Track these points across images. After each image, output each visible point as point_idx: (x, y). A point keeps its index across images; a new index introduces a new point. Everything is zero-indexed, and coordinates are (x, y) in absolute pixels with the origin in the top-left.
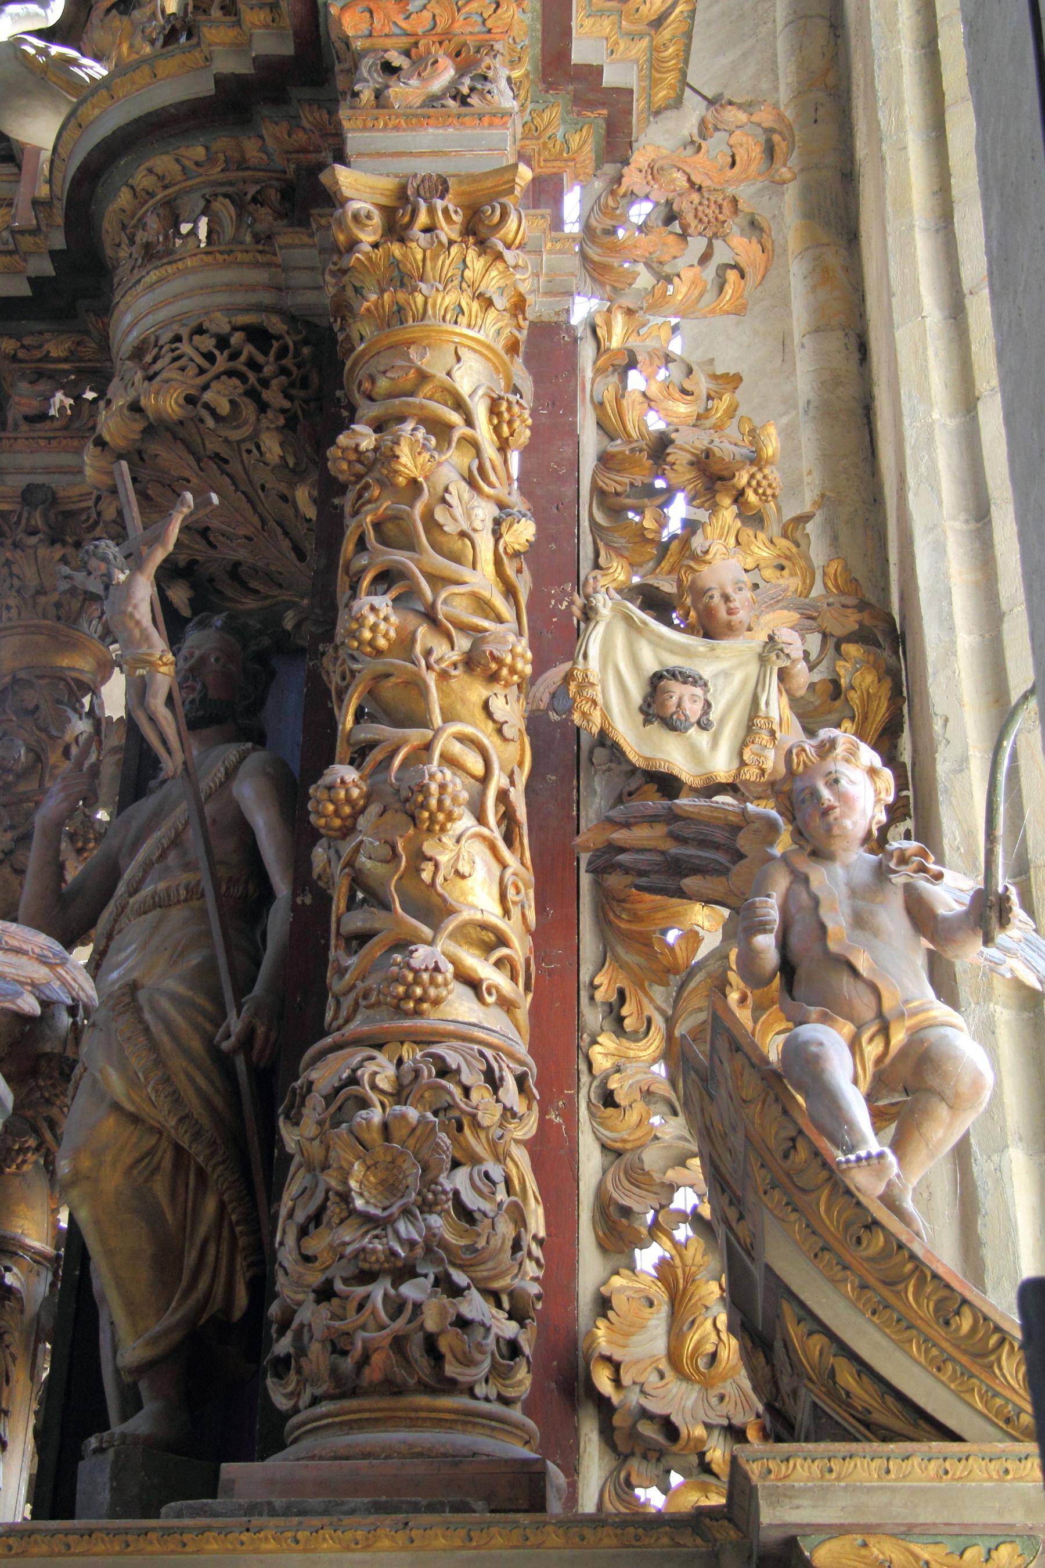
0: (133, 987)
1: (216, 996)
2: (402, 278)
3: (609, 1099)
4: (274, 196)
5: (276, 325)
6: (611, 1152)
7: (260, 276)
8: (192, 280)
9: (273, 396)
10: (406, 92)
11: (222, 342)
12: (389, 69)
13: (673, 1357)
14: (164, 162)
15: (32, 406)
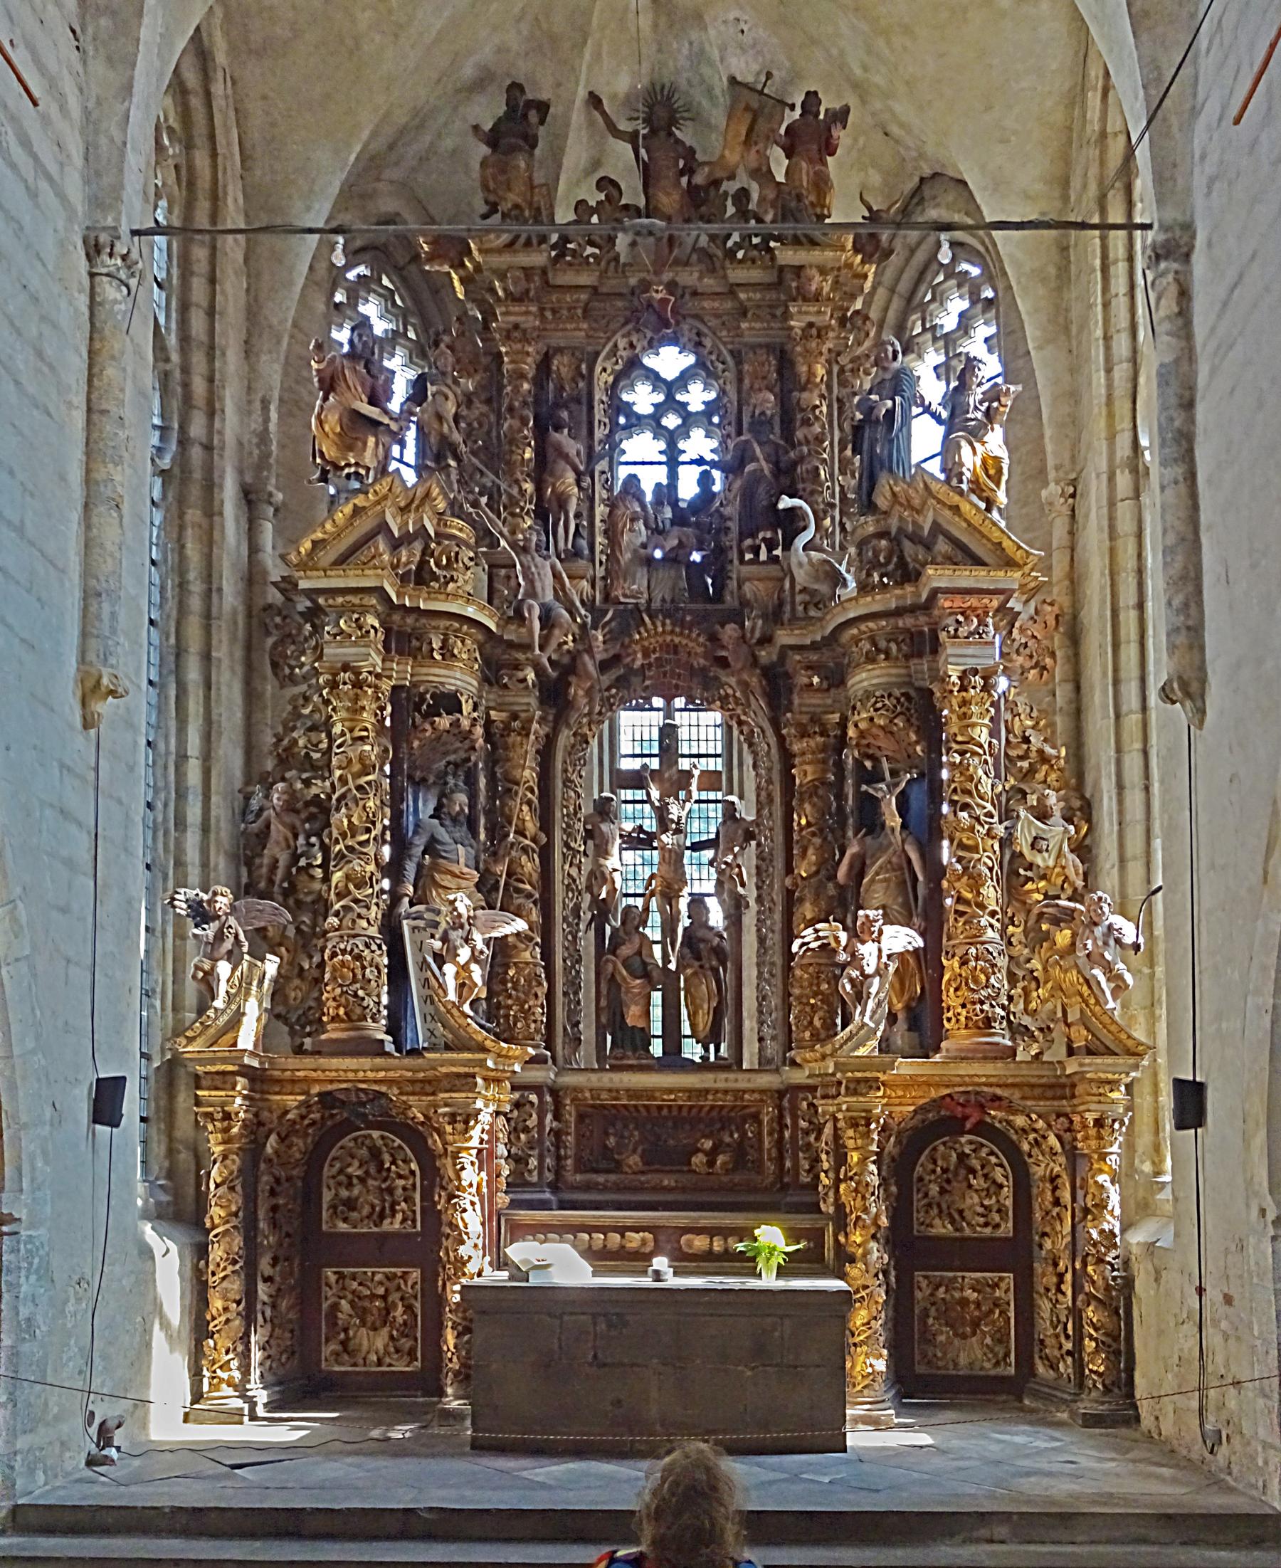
5: (913, 693)
7: (903, 671)
9: (913, 720)
11: (898, 700)
14: (871, 625)
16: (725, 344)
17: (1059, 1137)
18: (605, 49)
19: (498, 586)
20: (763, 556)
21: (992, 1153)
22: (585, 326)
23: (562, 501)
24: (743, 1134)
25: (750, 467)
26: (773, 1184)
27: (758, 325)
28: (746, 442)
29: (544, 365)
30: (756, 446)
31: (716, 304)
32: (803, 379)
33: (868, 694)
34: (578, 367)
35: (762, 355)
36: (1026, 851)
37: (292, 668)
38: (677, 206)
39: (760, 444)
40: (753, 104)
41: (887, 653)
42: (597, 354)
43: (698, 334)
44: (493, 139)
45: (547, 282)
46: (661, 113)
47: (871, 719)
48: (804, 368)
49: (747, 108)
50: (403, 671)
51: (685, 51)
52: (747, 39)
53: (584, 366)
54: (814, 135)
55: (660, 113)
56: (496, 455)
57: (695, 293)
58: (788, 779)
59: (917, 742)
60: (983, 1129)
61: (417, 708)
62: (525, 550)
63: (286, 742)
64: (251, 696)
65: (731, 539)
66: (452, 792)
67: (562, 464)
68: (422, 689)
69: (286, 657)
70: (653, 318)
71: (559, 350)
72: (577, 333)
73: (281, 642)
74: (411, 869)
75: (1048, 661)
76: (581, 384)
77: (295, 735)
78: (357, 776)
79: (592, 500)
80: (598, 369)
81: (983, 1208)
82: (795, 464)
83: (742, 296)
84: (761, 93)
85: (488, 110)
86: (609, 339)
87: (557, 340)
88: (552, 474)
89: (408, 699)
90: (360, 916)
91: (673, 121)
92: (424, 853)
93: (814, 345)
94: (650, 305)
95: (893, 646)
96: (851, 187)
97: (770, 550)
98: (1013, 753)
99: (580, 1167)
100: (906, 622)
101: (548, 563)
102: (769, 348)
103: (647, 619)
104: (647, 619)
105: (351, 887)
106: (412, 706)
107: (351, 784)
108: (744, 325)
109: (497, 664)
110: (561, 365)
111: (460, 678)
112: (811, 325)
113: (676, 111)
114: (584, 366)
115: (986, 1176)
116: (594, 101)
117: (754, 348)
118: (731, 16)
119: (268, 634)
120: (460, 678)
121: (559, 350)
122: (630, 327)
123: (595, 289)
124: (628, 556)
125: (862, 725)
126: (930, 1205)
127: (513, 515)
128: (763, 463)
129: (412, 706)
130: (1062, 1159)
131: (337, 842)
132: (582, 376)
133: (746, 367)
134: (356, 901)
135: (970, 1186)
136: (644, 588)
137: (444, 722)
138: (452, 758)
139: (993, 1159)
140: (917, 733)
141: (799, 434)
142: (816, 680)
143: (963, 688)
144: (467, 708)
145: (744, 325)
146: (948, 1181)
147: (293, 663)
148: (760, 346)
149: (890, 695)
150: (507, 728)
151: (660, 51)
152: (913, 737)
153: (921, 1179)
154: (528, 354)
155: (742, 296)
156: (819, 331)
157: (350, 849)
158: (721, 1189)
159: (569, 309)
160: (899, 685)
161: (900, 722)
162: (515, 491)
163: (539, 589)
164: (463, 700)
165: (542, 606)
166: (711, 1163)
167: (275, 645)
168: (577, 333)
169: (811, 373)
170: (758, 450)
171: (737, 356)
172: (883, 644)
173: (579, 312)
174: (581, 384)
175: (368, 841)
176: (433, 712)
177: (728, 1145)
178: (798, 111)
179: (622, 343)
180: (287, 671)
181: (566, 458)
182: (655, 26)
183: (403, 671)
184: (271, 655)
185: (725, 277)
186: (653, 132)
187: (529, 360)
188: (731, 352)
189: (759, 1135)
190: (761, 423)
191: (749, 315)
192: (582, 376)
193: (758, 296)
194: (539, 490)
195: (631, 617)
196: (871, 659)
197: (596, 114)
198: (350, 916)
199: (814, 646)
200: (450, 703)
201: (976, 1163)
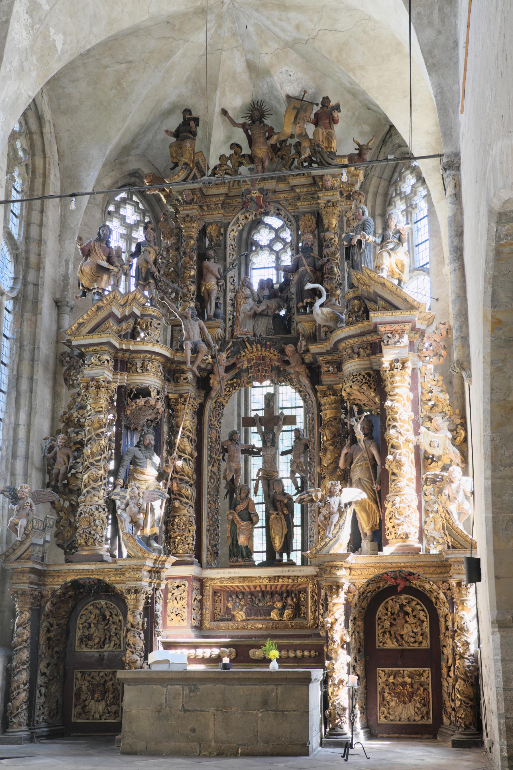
0: (360, 479)
1: (372, 480)
2: (393, 376)
3: (425, 495)
4: (369, 347)
5: (372, 373)
6: (426, 502)
7: (368, 362)
8: (357, 363)
9: (372, 386)
10: (391, 341)
11: (364, 376)
12: (388, 337)
13: (434, 528)
14: (351, 341)
15: (326, 369)
16: (290, 213)
17: (445, 593)
18: (227, 89)
19: (175, 335)
21: (418, 604)
22: (222, 211)
23: (209, 292)
24: (299, 600)
25: (301, 269)
26: (313, 625)
27: (305, 203)
28: (299, 257)
29: (203, 232)
30: (303, 259)
31: (286, 195)
32: (326, 226)
33: (350, 374)
34: (220, 231)
35: (308, 217)
38: (265, 154)
39: (306, 258)
40: (298, 105)
41: (359, 354)
42: (229, 223)
43: (278, 210)
44: (177, 134)
45: (203, 194)
46: (256, 113)
47: (351, 387)
48: (327, 221)
49: (294, 108)
50: (123, 379)
51: (265, 86)
52: (293, 78)
53: (222, 230)
54: (327, 115)
55: (256, 115)
56: (178, 276)
57: (275, 192)
59: (375, 396)
60: (410, 590)
61: (129, 396)
62: (186, 318)
63: (67, 415)
64: (55, 395)
66: (145, 434)
67: (210, 275)
68: (131, 387)
69: (70, 376)
70: (254, 205)
71: (211, 224)
72: (217, 215)
73: (69, 369)
76: (221, 238)
77: (72, 411)
78: (95, 429)
79: (225, 291)
80: (229, 230)
81: (413, 632)
82: (322, 266)
83: (298, 191)
84: (302, 100)
85: (175, 122)
86: (235, 216)
87: (209, 219)
90: (94, 495)
91: (262, 115)
93: (331, 210)
94: (251, 199)
95: (361, 350)
96: (345, 138)
99: (214, 618)
100: (368, 338)
101: (197, 323)
102: (312, 213)
103: (248, 345)
104: (248, 345)
105: (91, 481)
106: (126, 396)
107: (93, 433)
108: (299, 204)
109: (172, 372)
110: (212, 230)
111: (152, 380)
112: (329, 201)
113: (264, 112)
114: (222, 230)
115: (415, 616)
116: (224, 112)
117: (304, 214)
118: (284, 69)
119: (63, 365)
121: (211, 224)
122: (244, 210)
123: (227, 194)
125: (348, 390)
126: (384, 633)
127: (184, 301)
128: (307, 267)
129: (126, 396)
130: (447, 605)
132: (222, 234)
133: (300, 223)
134: (93, 488)
135: (406, 622)
137: (141, 401)
139: (419, 607)
140: (374, 392)
141: (325, 252)
143: (392, 369)
144: (153, 394)
145: (299, 204)
146: (395, 619)
147: (74, 378)
148: (307, 213)
149: (360, 374)
151: (254, 87)
152: (373, 394)
153: (380, 619)
154: (193, 227)
155: (298, 191)
156: (333, 203)
157: (92, 464)
158: (286, 627)
159: (215, 205)
160: (365, 369)
161: (364, 387)
162: (185, 290)
163: (192, 336)
164: (152, 390)
166: (281, 615)
167: (67, 370)
168: (217, 215)
169: (330, 223)
170: (304, 261)
171: (296, 218)
172: (356, 350)
173: (220, 205)
174: (221, 238)
175: (100, 459)
176: (136, 397)
177: (291, 605)
178: (320, 106)
179: (241, 217)
180: (71, 382)
181: (211, 272)
182: (251, 77)
183: (123, 379)
184: (64, 375)
185: (289, 183)
186: (254, 122)
187: (194, 230)
188: (294, 216)
189: (306, 600)
190: (307, 248)
191: (301, 199)
192: (222, 234)
193: (305, 190)
195: (240, 345)
196: (351, 357)
197: (226, 118)
198: (90, 495)
199: (328, 353)
200: (145, 392)
201: (409, 609)
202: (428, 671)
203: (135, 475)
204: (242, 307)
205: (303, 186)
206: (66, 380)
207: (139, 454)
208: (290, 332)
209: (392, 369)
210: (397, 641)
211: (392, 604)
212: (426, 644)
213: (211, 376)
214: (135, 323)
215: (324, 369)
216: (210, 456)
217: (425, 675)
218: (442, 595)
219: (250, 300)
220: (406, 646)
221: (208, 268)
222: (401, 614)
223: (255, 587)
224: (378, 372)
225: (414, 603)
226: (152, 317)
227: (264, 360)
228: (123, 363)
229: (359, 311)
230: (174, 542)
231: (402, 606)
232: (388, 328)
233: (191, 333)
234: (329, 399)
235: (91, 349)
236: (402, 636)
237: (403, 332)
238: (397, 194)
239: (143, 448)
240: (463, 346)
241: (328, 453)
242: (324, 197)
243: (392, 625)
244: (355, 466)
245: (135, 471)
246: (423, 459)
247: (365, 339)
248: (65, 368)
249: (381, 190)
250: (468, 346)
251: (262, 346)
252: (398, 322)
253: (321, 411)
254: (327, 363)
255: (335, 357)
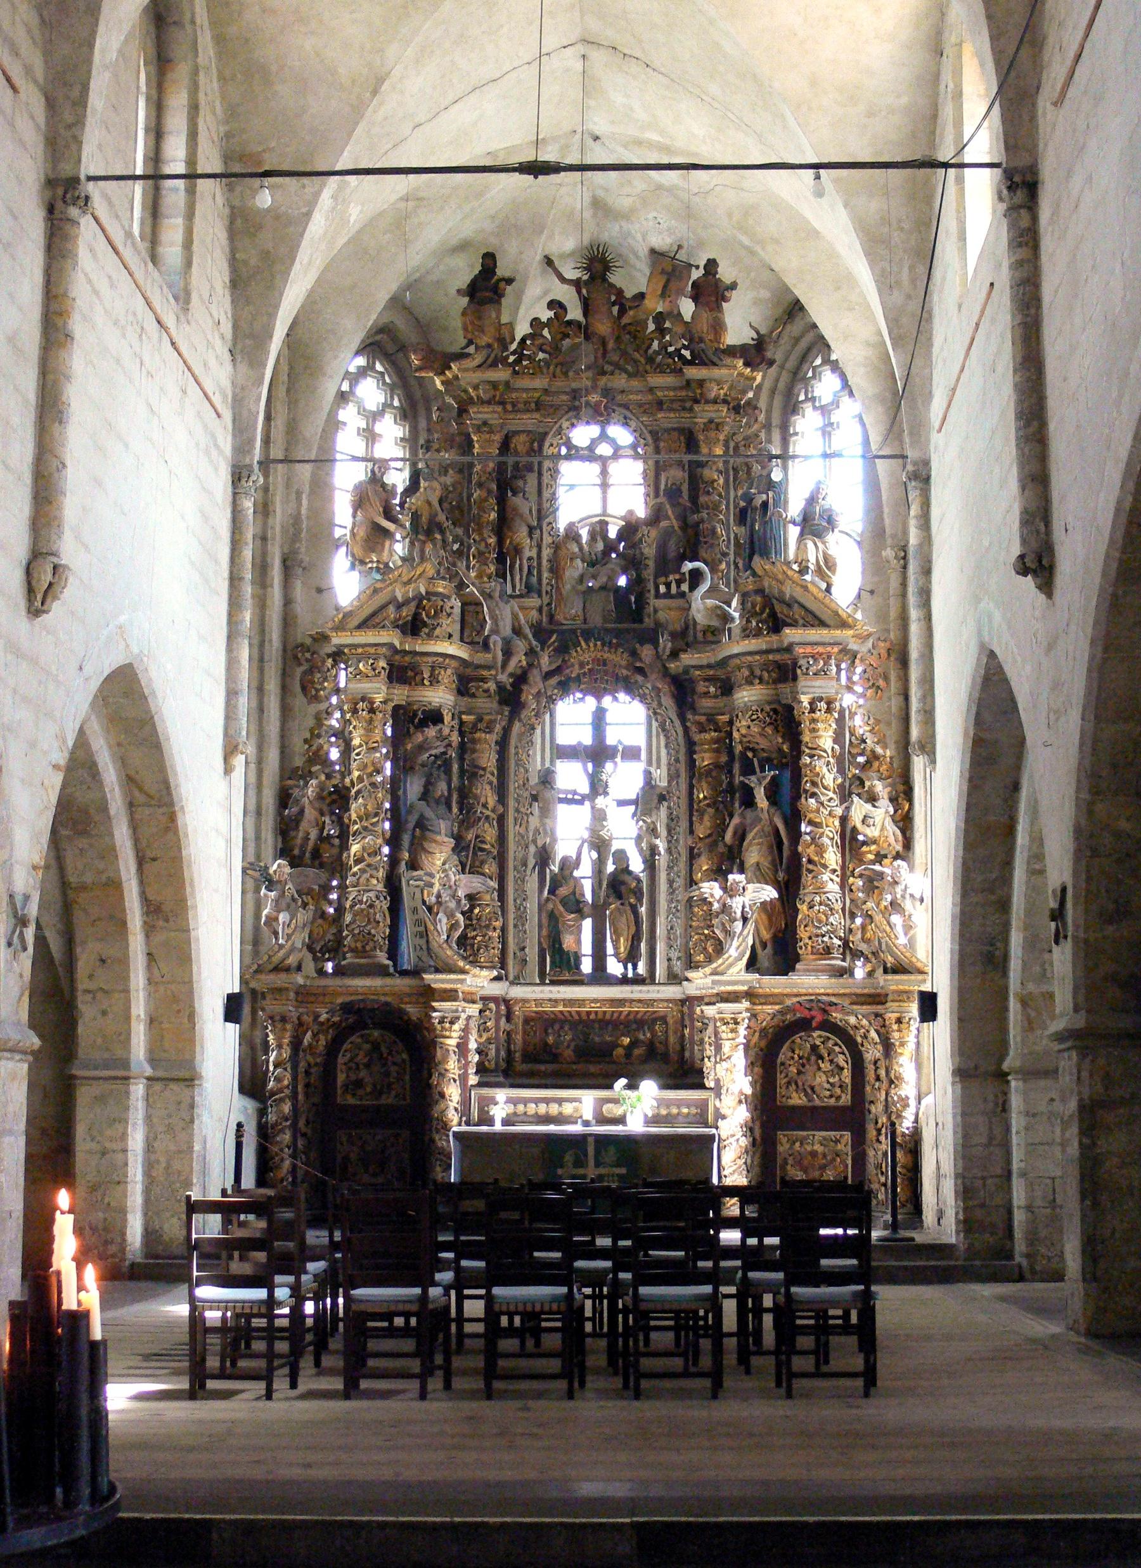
14: (749, 658)
20: (674, 590)
23: (517, 550)
33: (747, 708)
36: (859, 825)
37: (317, 691)
39: (673, 505)
42: (546, 434)
50: (401, 694)
58: (691, 763)
65: (649, 573)
74: (406, 839)
75: (881, 683)
79: (539, 547)
80: (547, 444)
82: (698, 524)
83: (660, 394)
88: (510, 528)
89: (404, 714)
92: (415, 827)
97: (678, 587)
98: (854, 751)
102: (680, 430)
109: (466, 682)
119: (300, 664)
120: (440, 696)
124: (568, 587)
125: (743, 731)
131: (355, 823)
136: (580, 613)
137: (431, 732)
138: (433, 752)
142: (712, 689)
144: (447, 718)
148: (674, 429)
150: (475, 728)
160: (769, 703)
161: (769, 730)
165: (504, 639)
172: (758, 672)
173: (533, 405)
194: (500, 542)
196: (750, 683)
198: (367, 875)
200: (434, 717)
202: (847, 1135)
203: (426, 845)
204: (567, 573)
205: (668, 388)
206: (304, 689)
207: (429, 813)
208: (641, 621)
209: (812, 711)
210: (806, 1095)
211: (802, 1043)
212: (846, 1099)
213: (525, 687)
214: (418, 607)
215: (701, 687)
216: (517, 811)
217: (843, 1141)
218: (873, 1034)
219: (579, 562)
220: (817, 1102)
221: (515, 509)
222: (813, 1058)
223: (588, 1013)
224: (790, 709)
225: (830, 1044)
226: (444, 597)
227: (605, 664)
228: (402, 671)
229: (762, 612)
230: (472, 945)
231: (814, 1048)
232: (809, 650)
233: (501, 624)
234: (707, 736)
235: (360, 650)
236: (812, 1088)
237: (829, 657)
238: (807, 399)
239: (433, 804)
240: (926, 723)
241: (706, 818)
242: (704, 414)
243: (799, 1073)
244: (750, 844)
245: (423, 838)
246: (850, 842)
247: (771, 657)
248: (302, 668)
249: (781, 385)
250: (933, 724)
251: (603, 645)
252: (823, 644)
253: (695, 752)
254: (705, 680)
255: (720, 673)
